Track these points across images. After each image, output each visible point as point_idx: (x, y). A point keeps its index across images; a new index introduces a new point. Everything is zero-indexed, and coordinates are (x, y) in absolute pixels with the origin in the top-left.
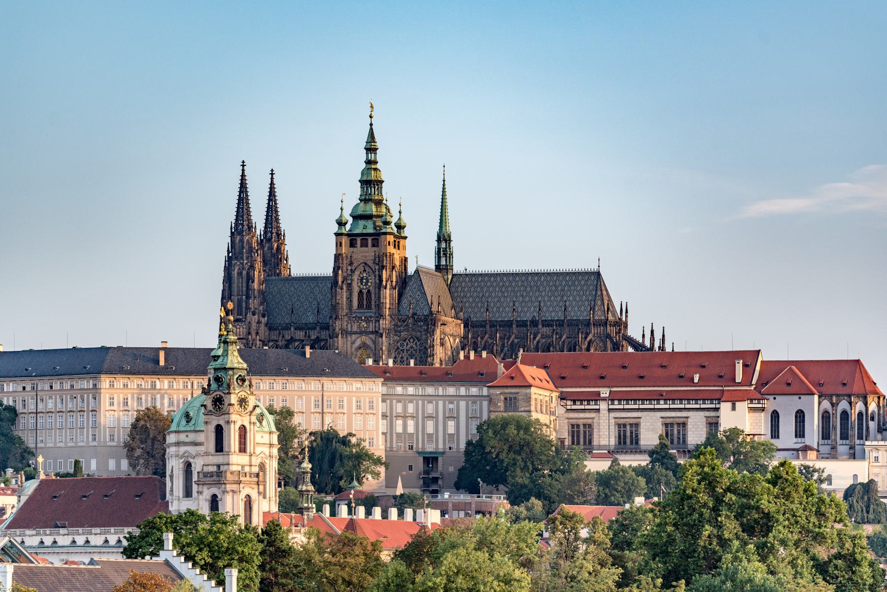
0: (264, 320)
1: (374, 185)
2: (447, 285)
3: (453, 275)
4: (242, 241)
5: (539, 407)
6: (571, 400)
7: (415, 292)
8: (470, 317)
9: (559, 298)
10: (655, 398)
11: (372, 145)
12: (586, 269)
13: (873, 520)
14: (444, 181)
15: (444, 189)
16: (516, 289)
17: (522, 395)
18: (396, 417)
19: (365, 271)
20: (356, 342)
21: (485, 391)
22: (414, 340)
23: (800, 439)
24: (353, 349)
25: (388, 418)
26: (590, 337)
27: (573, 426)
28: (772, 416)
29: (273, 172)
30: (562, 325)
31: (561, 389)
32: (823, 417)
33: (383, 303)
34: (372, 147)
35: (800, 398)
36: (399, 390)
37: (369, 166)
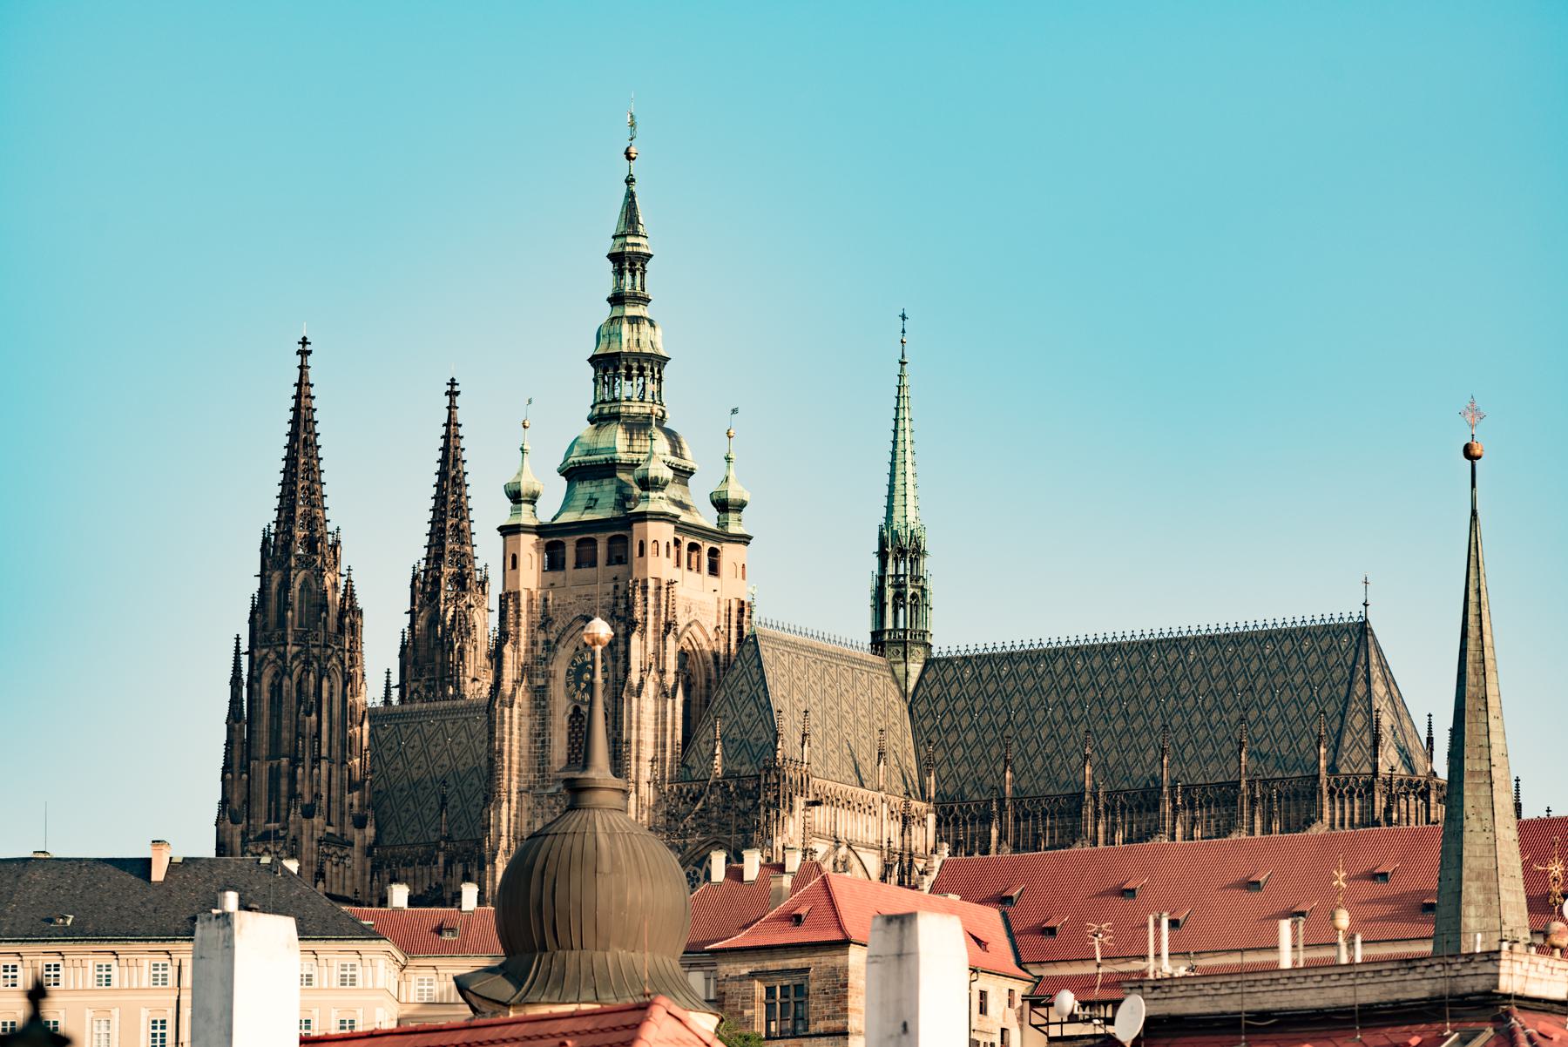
1: (629, 369)
2: (905, 695)
3: (929, 663)
4: (285, 585)
7: (739, 704)
8: (962, 790)
9: (1235, 715)
12: (1327, 617)
14: (903, 363)
16: (1110, 694)
17: (819, 978)
29: (456, 389)
30: (1234, 802)
31: (1036, 971)
33: (628, 742)
34: (628, 249)
37: (618, 312)
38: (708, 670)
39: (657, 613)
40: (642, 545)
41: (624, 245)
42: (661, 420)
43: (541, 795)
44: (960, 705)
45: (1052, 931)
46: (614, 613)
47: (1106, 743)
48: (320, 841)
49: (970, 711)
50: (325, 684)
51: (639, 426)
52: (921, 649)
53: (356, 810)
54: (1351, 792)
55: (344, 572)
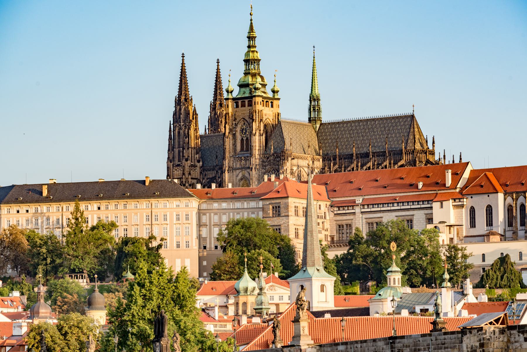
1: (252, 62)
2: (316, 132)
3: (321, 124)
4: (180, 109)
6: (337, 207)
9: (386, 136)
10: (391, 202)
11: (250, 35)
13: (505, 285)
14: (314, 57)
16: (359, 131)
18: (213, 225)
19: (244, 124)
20: (239, 175)
21: (261, 204)
22: (275, 171)
23: (489, 227)
24: (237, 181)
25: (208, 227)
26: (402, 162)
28: (470, 211)
30: (385, 155)
31: (332, 200)
32: (508, 210)
33: (253, 146)
34: (251, 36)
35: (488, 196)
36: (216, 205)
38: (271, 129)
39: (259, 117)
40: (255, 102)
41: (250, 35)
42: (259, 74)
43: (235, 158)
44: (328, 134)
45: (335, 191)
46: (249, 117)
47: (358, 142)
48: (189, 166)
49: (330, 135)
51: (254, 75)
52: (319, 121)
53: (198, 159)
54: (410, 153)
55: (193, 105)
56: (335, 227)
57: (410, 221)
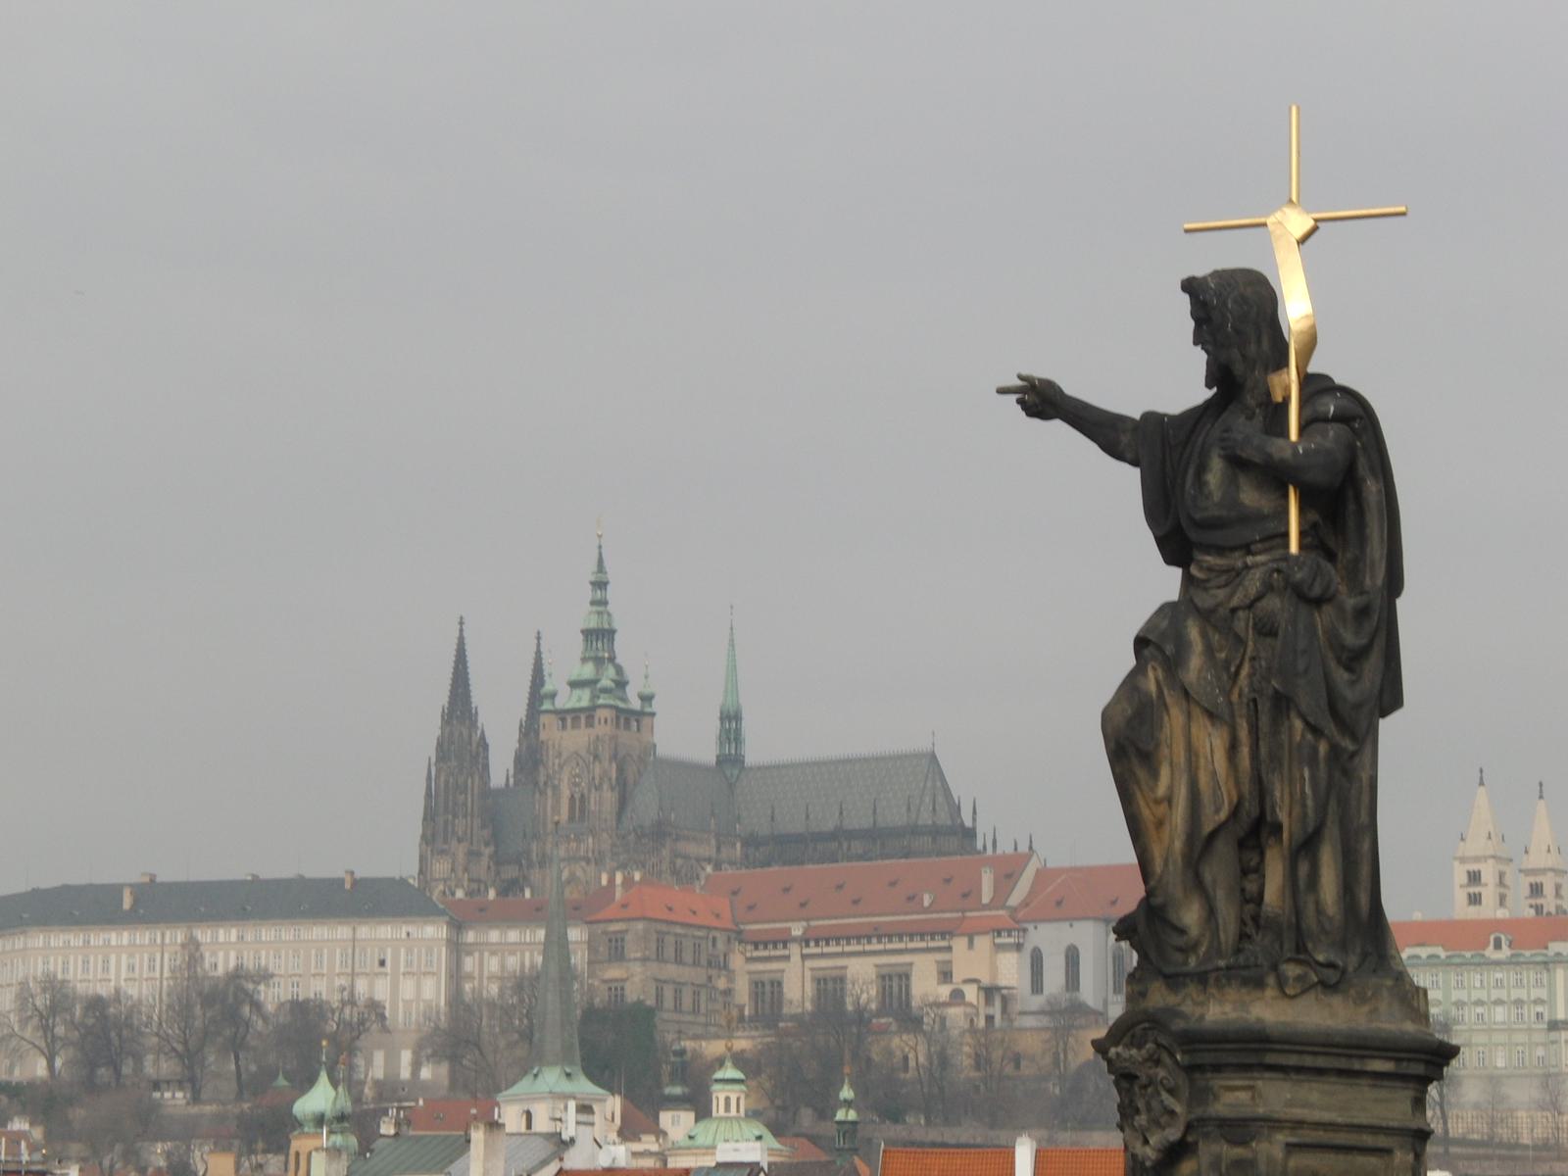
0: (488, 851)
5: (670, 952)
14: (732, 629)
15: (732, 641)
27: (756, 984)
32: (1114, 958)
35: (1071, 926)
42: (612, 659)
46: (588, 751)
50: (470, 781)
56: (747, 987)
57: (908, 977)
